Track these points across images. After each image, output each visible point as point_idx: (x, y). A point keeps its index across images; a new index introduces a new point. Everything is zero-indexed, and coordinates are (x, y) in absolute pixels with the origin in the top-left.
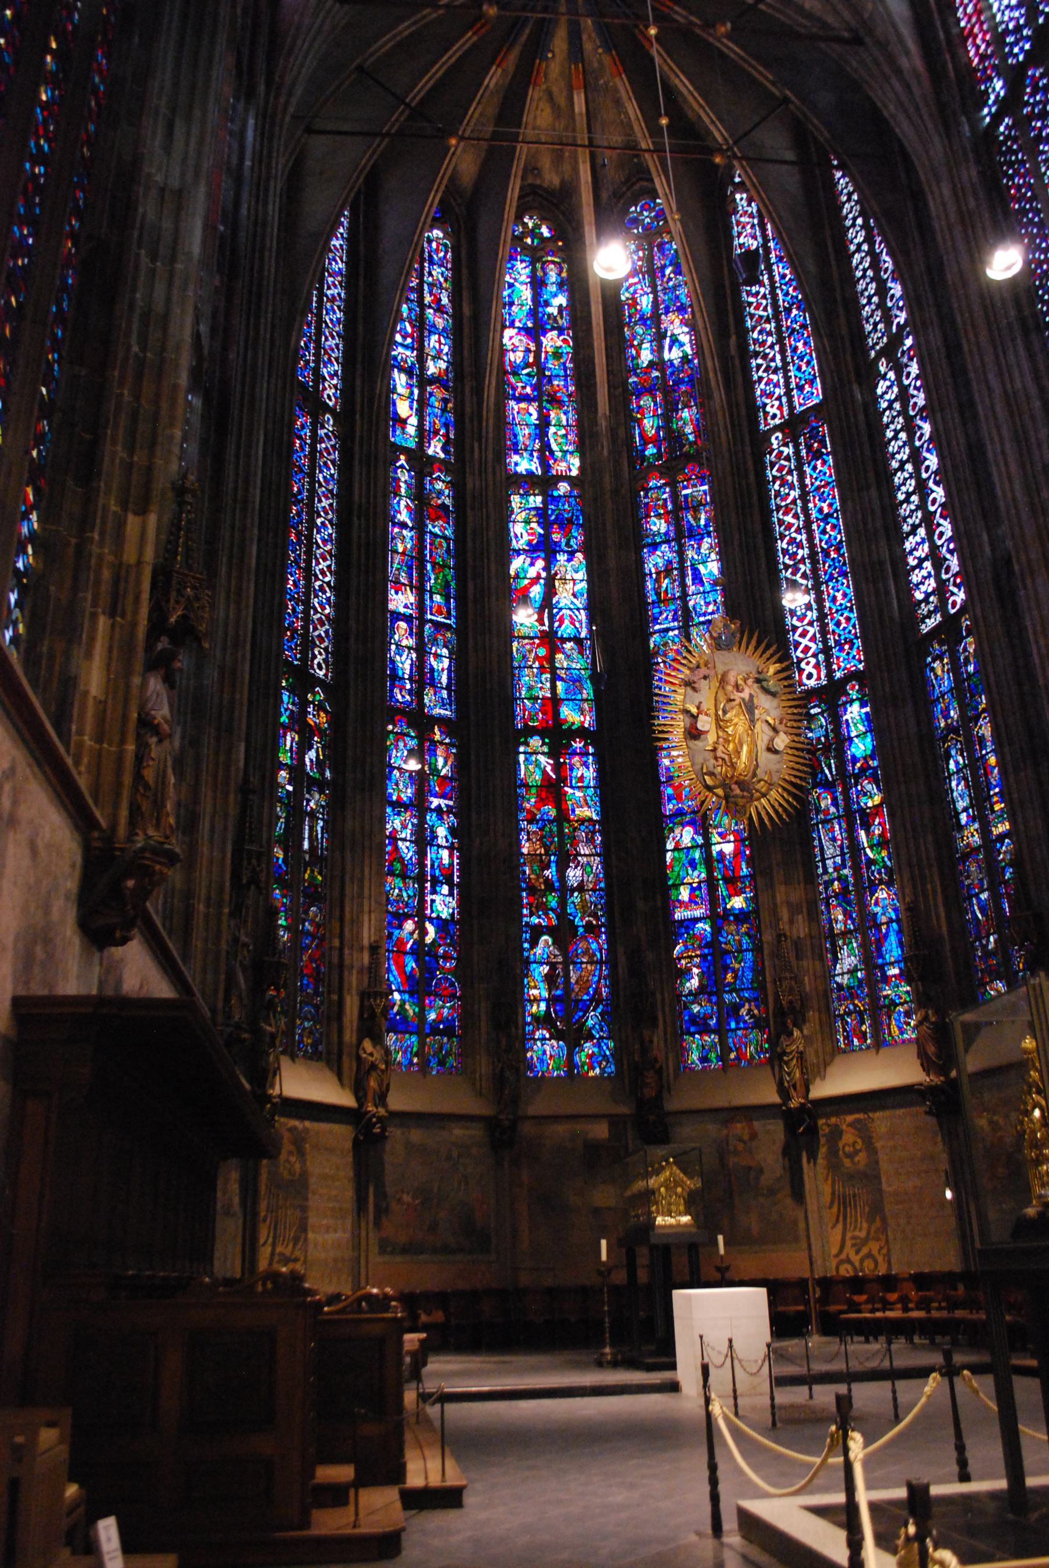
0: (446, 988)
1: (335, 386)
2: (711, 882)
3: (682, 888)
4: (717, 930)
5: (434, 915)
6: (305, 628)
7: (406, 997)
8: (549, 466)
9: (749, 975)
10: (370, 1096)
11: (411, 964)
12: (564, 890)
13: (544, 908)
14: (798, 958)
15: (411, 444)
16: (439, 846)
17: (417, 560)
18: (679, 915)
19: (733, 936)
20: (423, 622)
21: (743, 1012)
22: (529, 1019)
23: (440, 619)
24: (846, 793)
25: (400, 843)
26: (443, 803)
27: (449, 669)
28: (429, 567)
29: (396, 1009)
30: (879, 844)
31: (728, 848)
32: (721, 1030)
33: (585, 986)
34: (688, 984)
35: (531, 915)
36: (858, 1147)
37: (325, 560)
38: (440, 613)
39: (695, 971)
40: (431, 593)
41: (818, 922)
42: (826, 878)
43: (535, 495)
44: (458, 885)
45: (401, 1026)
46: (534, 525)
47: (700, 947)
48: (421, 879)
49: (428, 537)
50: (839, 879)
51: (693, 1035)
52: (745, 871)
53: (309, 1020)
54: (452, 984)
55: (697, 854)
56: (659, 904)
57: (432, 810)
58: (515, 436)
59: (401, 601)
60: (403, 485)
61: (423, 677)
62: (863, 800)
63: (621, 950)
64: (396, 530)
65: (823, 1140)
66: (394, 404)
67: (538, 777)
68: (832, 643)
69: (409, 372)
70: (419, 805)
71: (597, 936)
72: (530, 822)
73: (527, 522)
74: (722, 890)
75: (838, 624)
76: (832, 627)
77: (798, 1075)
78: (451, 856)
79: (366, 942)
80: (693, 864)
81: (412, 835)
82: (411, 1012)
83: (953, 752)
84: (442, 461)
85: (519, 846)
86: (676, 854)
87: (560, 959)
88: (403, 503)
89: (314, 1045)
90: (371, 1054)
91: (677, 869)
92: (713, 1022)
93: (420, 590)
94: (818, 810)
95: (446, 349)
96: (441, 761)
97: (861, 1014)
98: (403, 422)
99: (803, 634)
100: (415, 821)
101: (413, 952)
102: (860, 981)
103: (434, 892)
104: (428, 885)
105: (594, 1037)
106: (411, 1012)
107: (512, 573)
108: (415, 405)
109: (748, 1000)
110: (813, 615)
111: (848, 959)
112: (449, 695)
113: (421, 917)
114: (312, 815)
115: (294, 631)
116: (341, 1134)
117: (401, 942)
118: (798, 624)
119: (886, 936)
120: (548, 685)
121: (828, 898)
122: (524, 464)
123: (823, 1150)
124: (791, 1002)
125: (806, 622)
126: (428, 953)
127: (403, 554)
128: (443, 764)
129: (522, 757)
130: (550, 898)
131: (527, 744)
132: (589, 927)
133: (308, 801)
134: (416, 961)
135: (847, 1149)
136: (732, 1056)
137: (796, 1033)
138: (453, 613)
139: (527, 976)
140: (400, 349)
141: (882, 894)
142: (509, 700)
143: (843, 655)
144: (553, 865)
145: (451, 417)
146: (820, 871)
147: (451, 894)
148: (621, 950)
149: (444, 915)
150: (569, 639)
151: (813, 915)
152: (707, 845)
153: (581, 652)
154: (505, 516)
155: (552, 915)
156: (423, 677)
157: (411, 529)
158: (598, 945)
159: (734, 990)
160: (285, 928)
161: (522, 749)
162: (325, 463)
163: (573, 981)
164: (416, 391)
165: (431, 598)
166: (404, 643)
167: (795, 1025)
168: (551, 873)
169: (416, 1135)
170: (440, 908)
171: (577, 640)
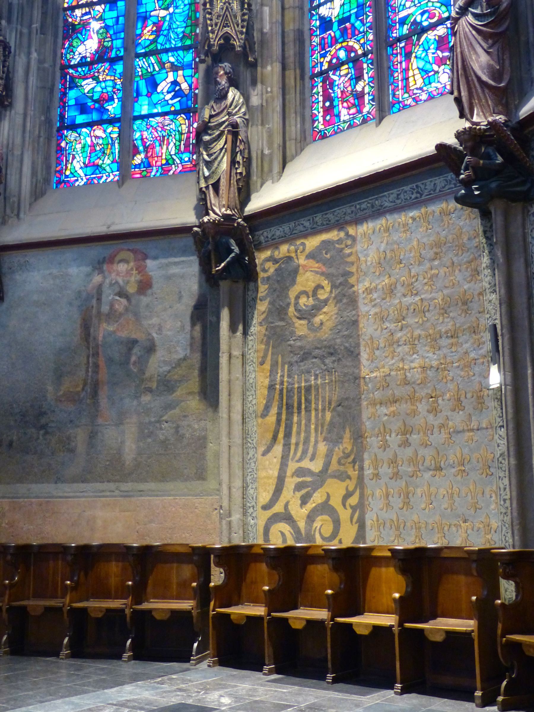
36: (323, 295)
65: (263, 289)
77: (224, 165)
123: (262, 307)
124: (227, 38)
136: (138, 159)
137: (233, 94)
167: (234, 82)
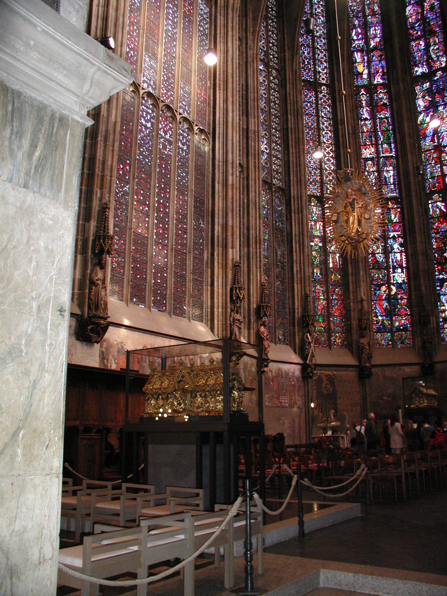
0: (403, 312)
1: (326, 73)
5: (395, 282)
6: (322, 179)
7: (384, 318)
8: (432, 67)
10: (363, 361)
11: (385, 304)
15: (366, 83)
16: (395, 253)
17: (374, 132)
20: (378, 157)
22: (441, 320)
23: (388, 154)
25: (377, 255)
26: (395, 234)
27: (394, 175)
28: (380, 133)
29: (380, 323)
35: (439, 275)
37: (328, 147)
38: (387, 151)
40: (382, 144)
43: (426, 83)
44: (406, 267)
45: (383, 329)
46: (427, 97)
48: (387, 268)
49: (378, 121)
53: (338, 333)
54: (405, 310)
57: (390, 238)
58: (415, 58)
59: (368, 152)
60: (364, 102)
61: (381, 181)
64: (363, 123)
66: (356, 68)
69: (361, 51)
70: (385, 238)
72: (436, 234)
73: (423, 97)
78: (401, 256)
79: (359, 299)
81: (382, 250)
82: (387, 324)
84: (381, 84)
88: (365, 110)
89: (342, 342)
90: (362, 343)
93: (376, 145)
95: (379, 32)
96: (393, 216)
98: (362, 74)
100: (383, 244)
101: (386, 299)
103: (394, 272)
104: (391, 270)
106: (387, 324)
107: (419, 123)
108: (366, 64)
112: (395, 187)
113: (389, 283)
114: (334, 253)
115: (317, 181)
116: (352, 374)
117: (380, 296)
120: (439, 170)
122: (419, 70)
126: (393, 299)
127: (367, 131)
128: (394, 218)
129: (430, 206)
131: (432, 199)
133: (330, 247)
134: (387, 303)
138: (394, 150)
140: (357, 42)
145: (383, 63)
147: (402, 272)
149: (400, 281)
154: (414, 97)
156: (381, 181)
157: (370, 120)
160: (324, 300)
161: (430, 202)
162: (325, 108)
164: (366, 58)
165: (382, 146)
166: (371, 170)
169: (388, 372)
170: (397, 279)
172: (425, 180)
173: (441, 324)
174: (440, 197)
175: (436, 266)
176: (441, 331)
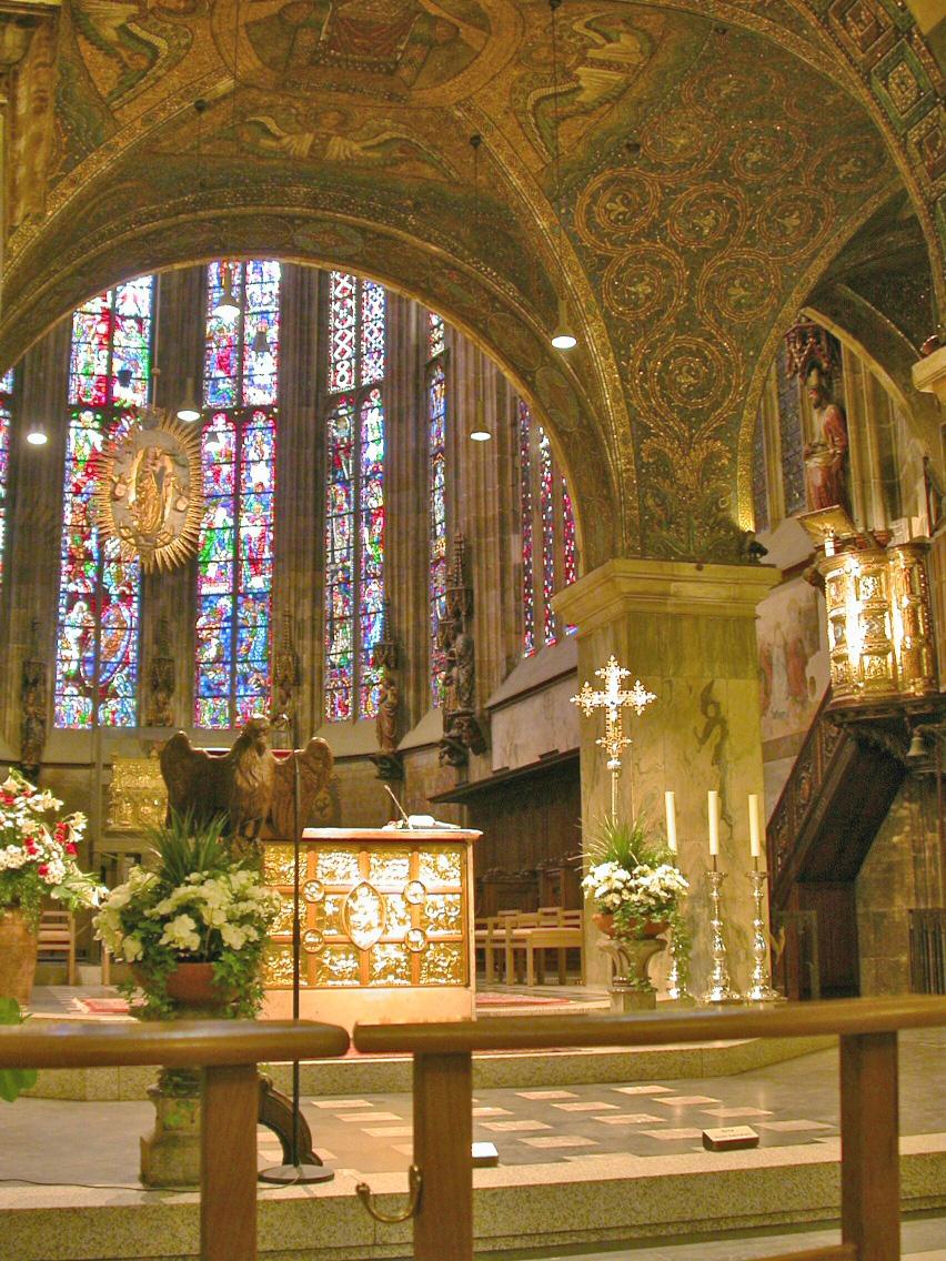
2: (236, 561)
3: (210, 565)
4: (236, 607)
9: (260, 649)
12: (103, 560)
13: (82, 575)
14: (301, 637)
18: (206, 589)
19: (252, 613)
21: (252, 681)
24: (358, 490)
30: (378, 543)
31: (255, 532)
32: (232, 697)
33: (113, 650)
34: (206, 654)
35: (70, 581)
39: (215, 641)
41: (322, 606)
42: (333, 567)
47: (220, 620)
50: (342, 570)
51: (205, 698)
52: (267, 554)
55: (227, 534)
56: (186, 579)
62: (371, 500)
63: (147, 618)
67: (87, 451)
68: (364, 350)
71: (129, 605)
74: (246, 569)
75: (371, 333)
76: (366, 334)
80: (221, 543)
83: (439, 470)
85: (61, 515)
86: (208, 533)
87: (93, 624)
91: (207, 547)
92: (225, 689)
94: (334, 506)
97: (346, 688)
99: (342, 338)
102: (349, 662)
105: (118, 696)
109: (256, 671)
110: (352, 321)
111: (342, 641)
118: (339, 326)
119: (370, 627)
120: (104, 362)
121: (332, 586)
125: (346, 325)
129: (72, 432)
130: (88, 567)
132: (124, 598)
135: (320, 804)
136: (238, 719)
139: (61, 638)
141: (374, 586)
142: (64, 378)
143: (371, 363)
144: (94, 537)
146: (329, 560)
148: (147, 618)
150: (130, 318)
151: (317, 600)
152: (236, 527)
153: (140, 331)
155: (88, 582)
158: (129, 614)
159: (246, 661)
161: (73, 423)
163: (103, 644)
168: (91, 544)
171: (139, 320)
172: (69, 374)
173: (58, 685)
174: (95, 420)
175: (64, 562)
176: (57, 701)
